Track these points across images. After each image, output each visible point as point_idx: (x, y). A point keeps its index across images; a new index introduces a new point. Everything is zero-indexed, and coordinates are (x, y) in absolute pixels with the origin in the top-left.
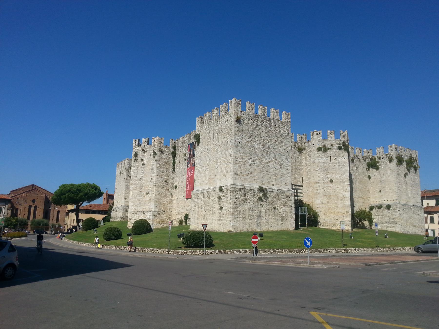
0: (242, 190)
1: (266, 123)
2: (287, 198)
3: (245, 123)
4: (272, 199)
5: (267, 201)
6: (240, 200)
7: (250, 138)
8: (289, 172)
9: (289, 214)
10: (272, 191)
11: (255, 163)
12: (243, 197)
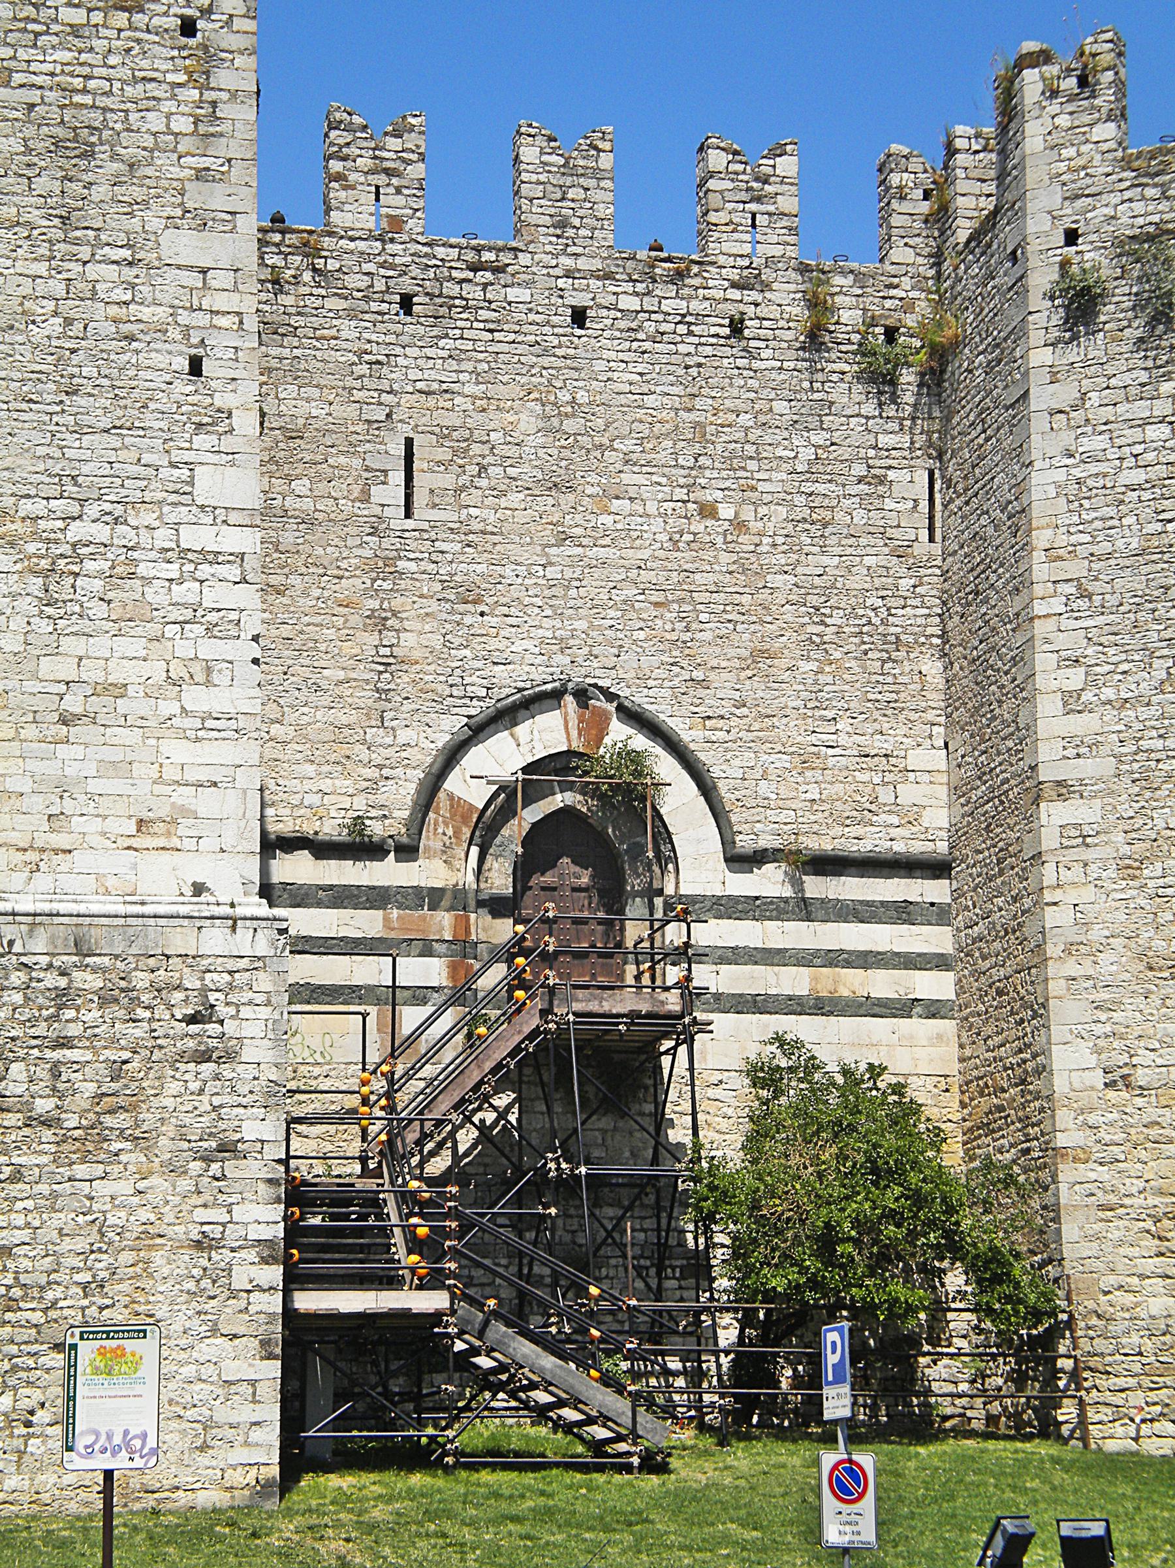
2: (139, 1031)
8: (209, 649)
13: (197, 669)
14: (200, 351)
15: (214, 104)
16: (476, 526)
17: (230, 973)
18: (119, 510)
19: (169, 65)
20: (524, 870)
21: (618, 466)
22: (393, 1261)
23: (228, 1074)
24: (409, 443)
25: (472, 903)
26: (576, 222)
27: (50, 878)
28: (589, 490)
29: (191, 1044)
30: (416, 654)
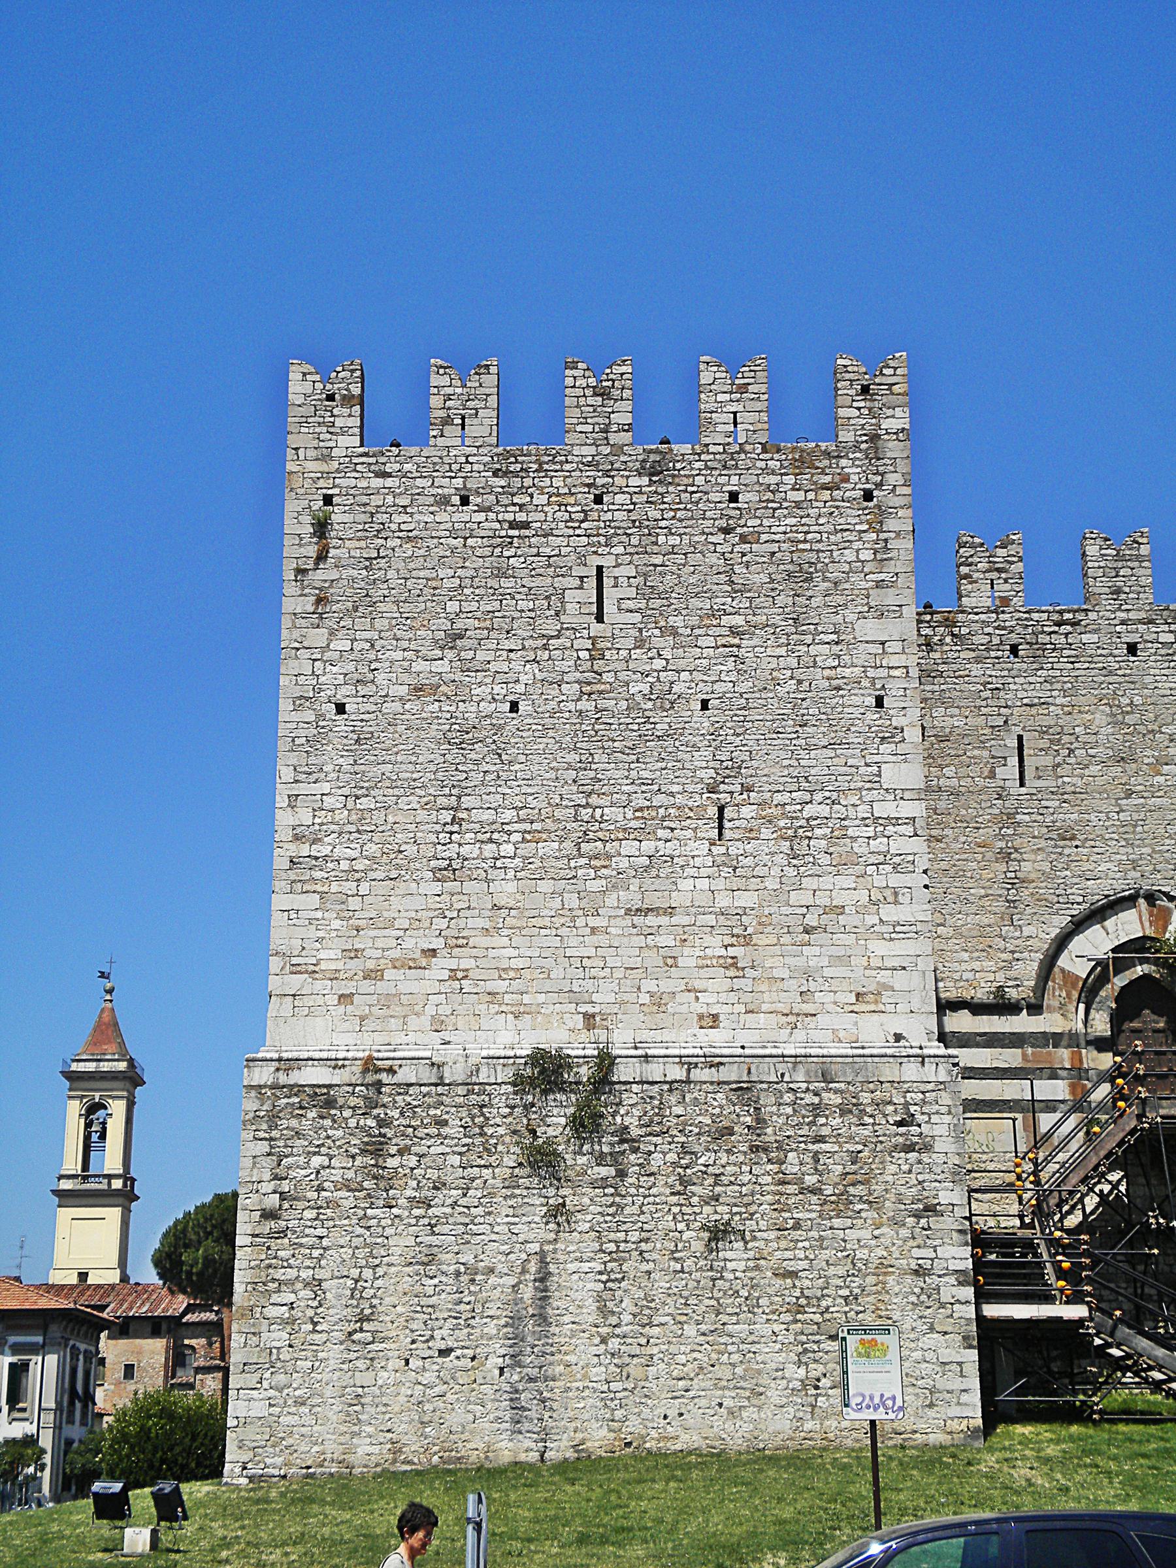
0: (341, 1101)
1: (619, 498)
3: (390, 543)
4: (685, 1150)
5: (622, 1174)
6: (320, 1189)
7: (450, 654)
8: (895, 880)
9: (900, 1287)
10: (678, 1073)
11: (507, 849)
12: (353, 1157)
13: (888, 893)
14: (882, 693)
15: (886, 541)
16: (1069, 789)
17: (923, 1093)
18: (834, 795)
19: (857, 520)
20: (1117, 1019)
21: (1166, 743)
22: (1048, 1285)
23: (926, 1160)
24: (1020, 738)
25: (1083, 1043)
26: (1127, 590)
27: (804, 1032)
28: (1146, 761)
29: (901, 1140)
30: (1033, 876)
